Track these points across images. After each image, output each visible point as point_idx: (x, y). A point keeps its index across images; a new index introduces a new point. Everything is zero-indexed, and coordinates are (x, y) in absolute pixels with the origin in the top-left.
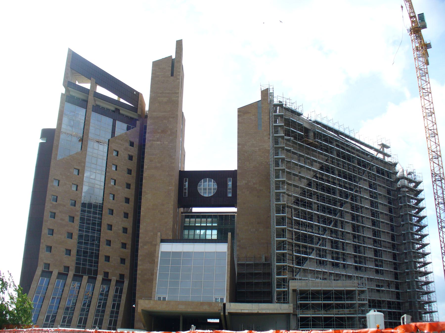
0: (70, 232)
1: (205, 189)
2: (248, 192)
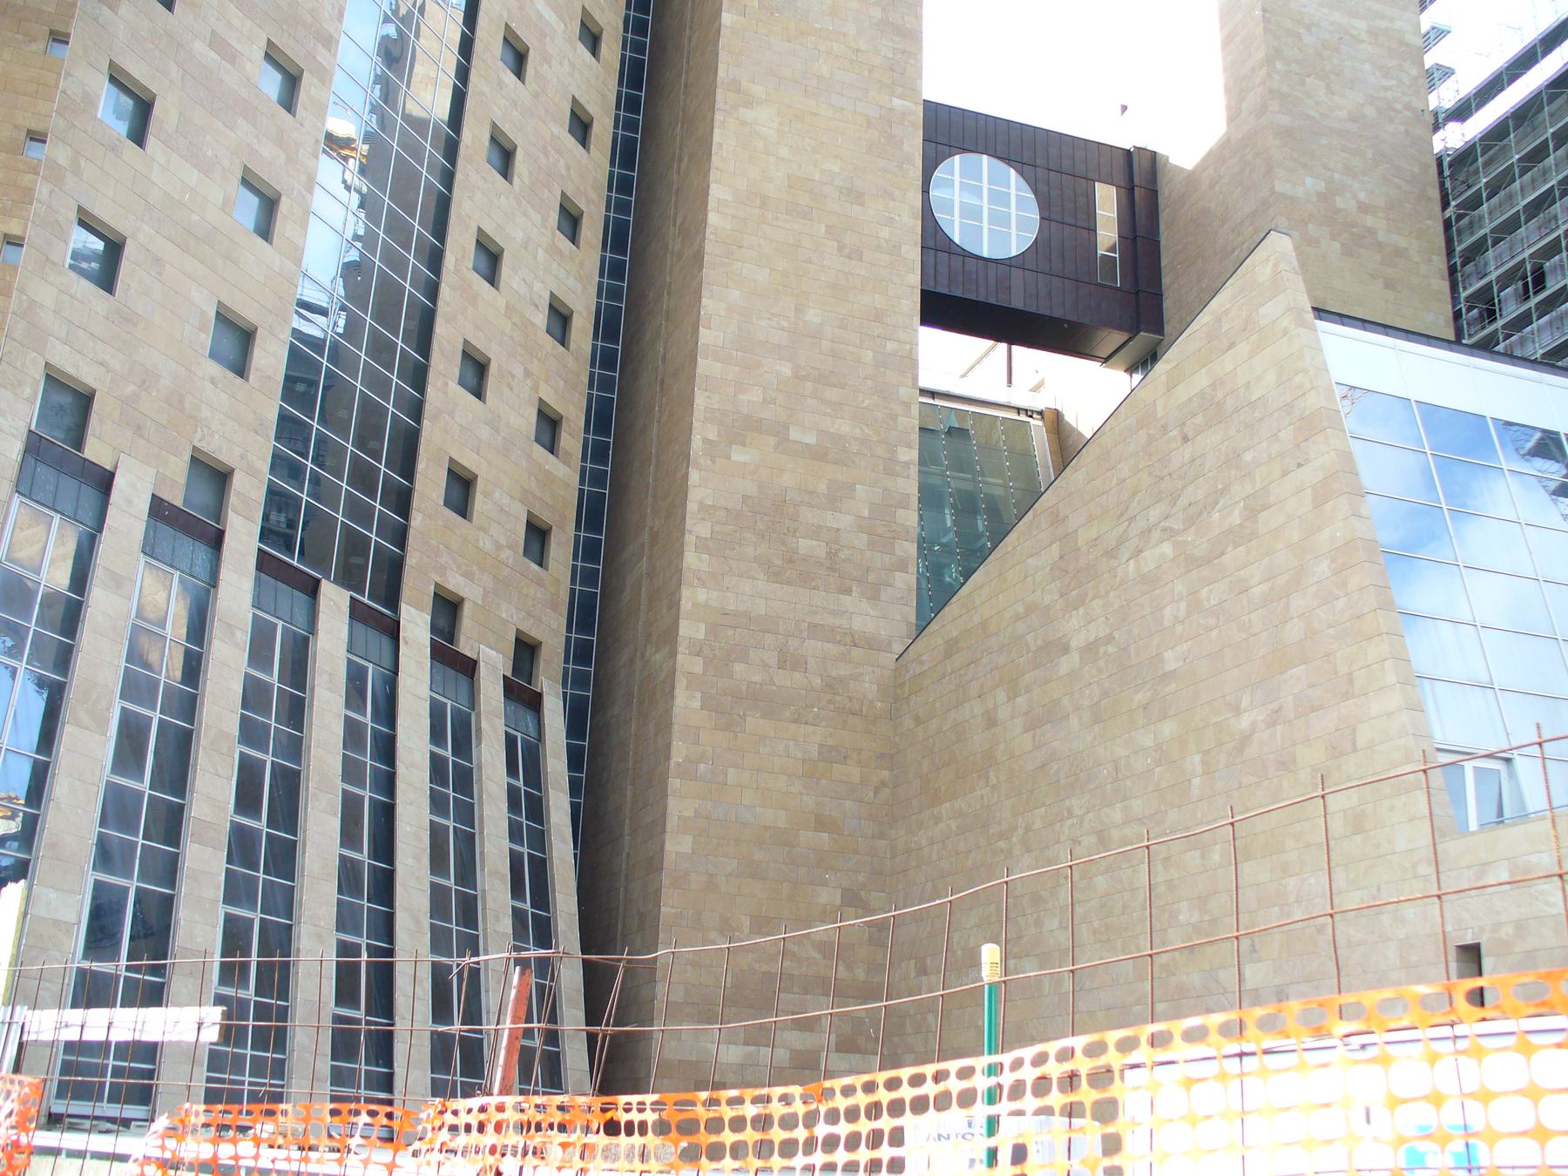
1: (972, 213)
2: (1337, 245)
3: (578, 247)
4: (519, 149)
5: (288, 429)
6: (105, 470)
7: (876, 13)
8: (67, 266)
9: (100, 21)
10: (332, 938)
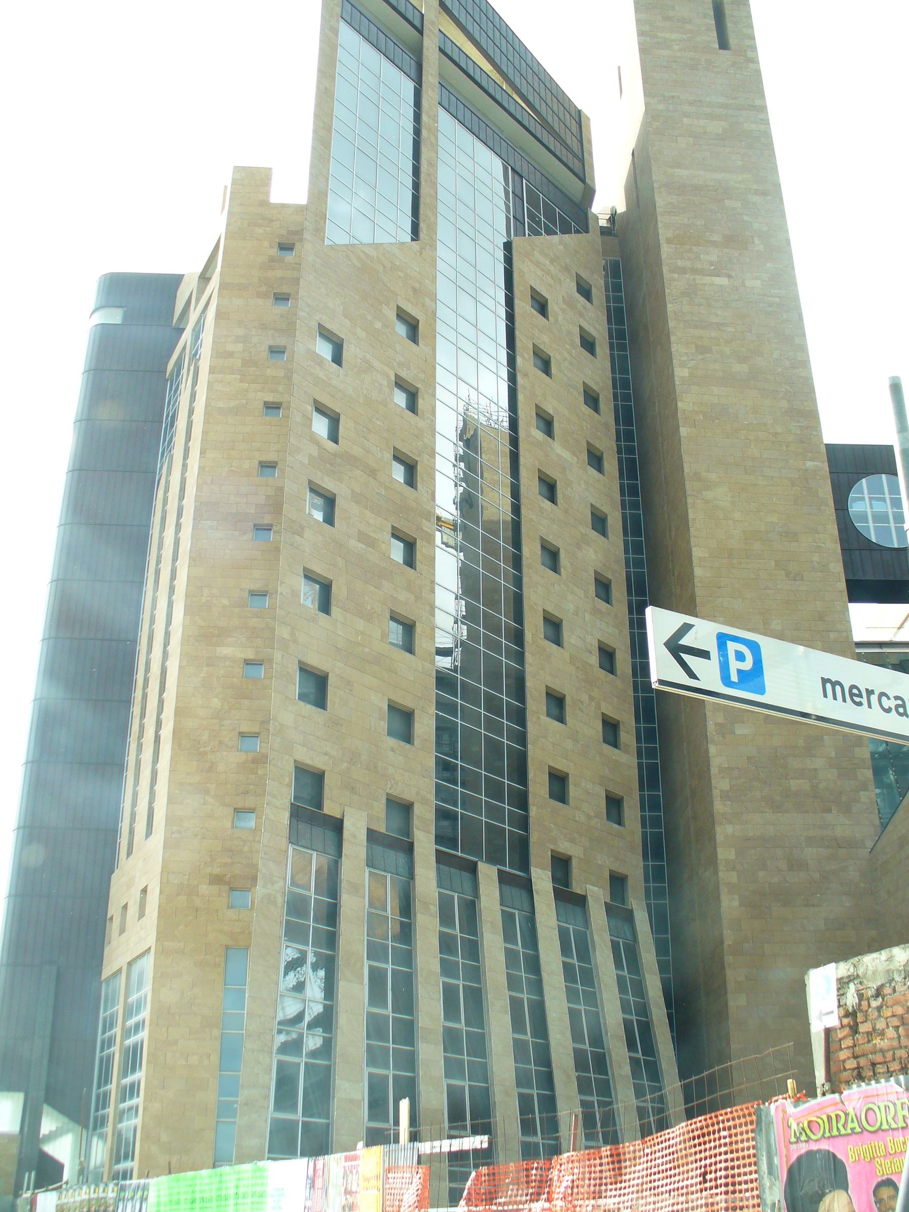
0: (401, 610)
3: (612, 605)
4: (561, 550)
5: (445, 768)
6: (337, 818)
7: (784, 404)
8: (297, 698)
9: (295, 545)
10: (515, 1092)
